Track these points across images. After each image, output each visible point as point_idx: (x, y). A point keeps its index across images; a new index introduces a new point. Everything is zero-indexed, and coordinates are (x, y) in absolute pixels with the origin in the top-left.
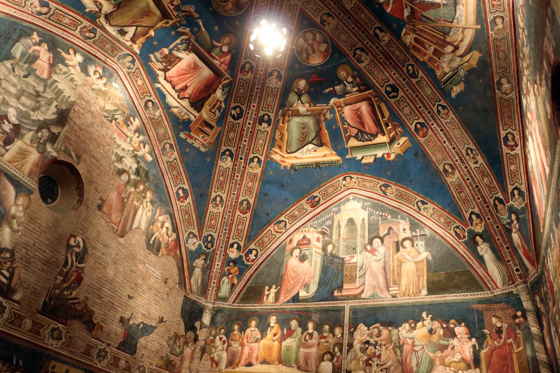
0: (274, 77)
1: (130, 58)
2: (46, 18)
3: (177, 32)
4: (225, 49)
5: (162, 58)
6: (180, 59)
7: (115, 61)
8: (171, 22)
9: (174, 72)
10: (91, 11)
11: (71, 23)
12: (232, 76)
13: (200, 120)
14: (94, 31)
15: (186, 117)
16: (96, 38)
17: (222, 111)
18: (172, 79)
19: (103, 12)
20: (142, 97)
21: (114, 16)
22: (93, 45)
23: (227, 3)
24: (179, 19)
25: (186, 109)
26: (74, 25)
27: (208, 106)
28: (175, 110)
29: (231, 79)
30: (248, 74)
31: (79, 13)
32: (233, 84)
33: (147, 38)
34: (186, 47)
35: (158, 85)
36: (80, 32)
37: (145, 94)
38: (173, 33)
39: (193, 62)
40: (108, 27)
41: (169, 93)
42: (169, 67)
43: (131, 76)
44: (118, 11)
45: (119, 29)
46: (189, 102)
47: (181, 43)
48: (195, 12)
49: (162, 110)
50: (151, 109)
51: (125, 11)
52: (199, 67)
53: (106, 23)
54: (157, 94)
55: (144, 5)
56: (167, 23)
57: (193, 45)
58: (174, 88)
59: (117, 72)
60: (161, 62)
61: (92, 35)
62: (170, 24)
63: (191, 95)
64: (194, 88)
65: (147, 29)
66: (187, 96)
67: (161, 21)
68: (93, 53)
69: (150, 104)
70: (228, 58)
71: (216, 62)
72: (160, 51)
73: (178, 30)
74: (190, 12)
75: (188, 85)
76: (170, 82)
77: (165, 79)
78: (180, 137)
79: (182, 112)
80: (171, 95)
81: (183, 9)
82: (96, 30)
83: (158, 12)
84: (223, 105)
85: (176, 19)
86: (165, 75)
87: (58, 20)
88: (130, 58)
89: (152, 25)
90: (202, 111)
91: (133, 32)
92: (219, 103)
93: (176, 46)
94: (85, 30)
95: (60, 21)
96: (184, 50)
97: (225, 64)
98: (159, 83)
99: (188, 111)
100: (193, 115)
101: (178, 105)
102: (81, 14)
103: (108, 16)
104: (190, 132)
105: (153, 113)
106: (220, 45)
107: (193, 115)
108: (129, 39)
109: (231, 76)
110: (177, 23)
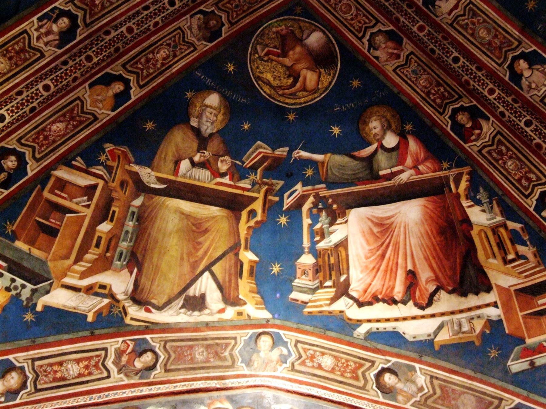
0: (527, 74)
1: (265, 342)
2: (29, 394)
3: (287, 212)
4: (391, 141)
5: (314, 279)
6: (343, 244)
7: (246, 372)
8: (258, 206)
9: (361, 276)
10: (99, 314)
11: (87, 367)
12: (459, 165)
13: (510, 299)
14: (144, 347)
15: (479, 326)
16: (162, 356)
17: (526, 238)
18: (372, 290)
19: (120, 297)
20: (361, 383)
21: (148, 284)
22: (171, 376)
23: (301, 79)
24: (266, 187)
25: (461, 311)
26: (96, 366)
27: (491, 260)
28: (444, 337)
29: (466, 169)
30: (481, 128)
31: (81, 334)
32: (481, 173)
33: (251, 273)
34: (328, 215)
35: (363, 329)
36: (120, 371)
37: (360, 372)
38: (283, 220)
39: (370, 224)
40: (156, 317)
41: (397, 320)
42: (343, 278)
43: (303, 369)
44: (145, 271)
45: (180, 301)
46: (450, 292)
47: (315, 219)
48: (273, 150)
49: (420, 362)
50: (400, 386)
51: (155, 260)
52: (389, 218)
53: (148, 311)
54: (379, 346)
55: (176, 221)
56: (253, 213)
57: (336, 198)
58: (394, 302)
59: (268, 387)
60: (321, 286)
61: (148, 358)
62: (259, 211)
63: (437, 279)
64: (427, 259)
65: (231, 255)
66: (432, 288)
67: (238, 219)
68: (185, 388)
69: (388, 379)
70: (413, 145)
71: (404, 177)
72: (299, 272)
73: (285, 207)
74: (265, 158)
75: (410, 267)
76: (375, 299)
77: (361, 304)
78: (517, 374)
79: (460, 325)
80: (405, 319)
81: (248, 163)
82: (145, 340)
83: (214, 210)
84: (512, 225)
85: (259, 192)
86: (352, 298)
87: (55, 380)
88: (265, 342)
89: (231, 244)
90: (493, 281)
91: (214, 286)
92: (502, 230)
93: (312, 234)
94: (125, 359)
95: (63, 379)
96: (331, 224)
97: (422, 162)
98: (359, 322)
99: (470, 309)
100: (487, 305)
101: (436, 322)
102: (87, 333)
103: (137, 297)
104: (522, 341)
105: (414, 389)
106: (375, 146)
107: (487, 305)
108: (222, 305)
109: (458, 166)
110: (270, 197)
